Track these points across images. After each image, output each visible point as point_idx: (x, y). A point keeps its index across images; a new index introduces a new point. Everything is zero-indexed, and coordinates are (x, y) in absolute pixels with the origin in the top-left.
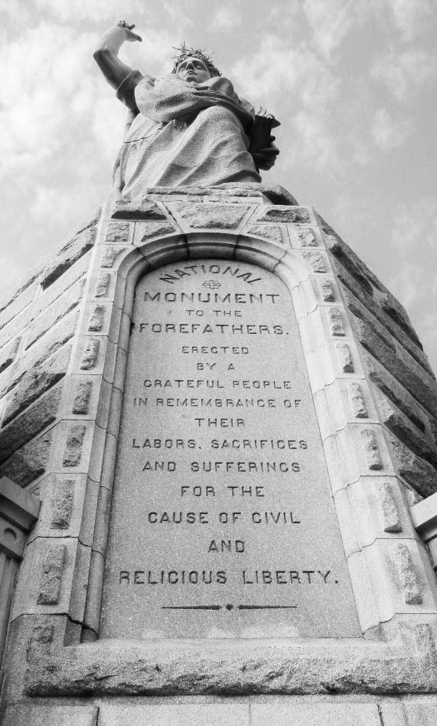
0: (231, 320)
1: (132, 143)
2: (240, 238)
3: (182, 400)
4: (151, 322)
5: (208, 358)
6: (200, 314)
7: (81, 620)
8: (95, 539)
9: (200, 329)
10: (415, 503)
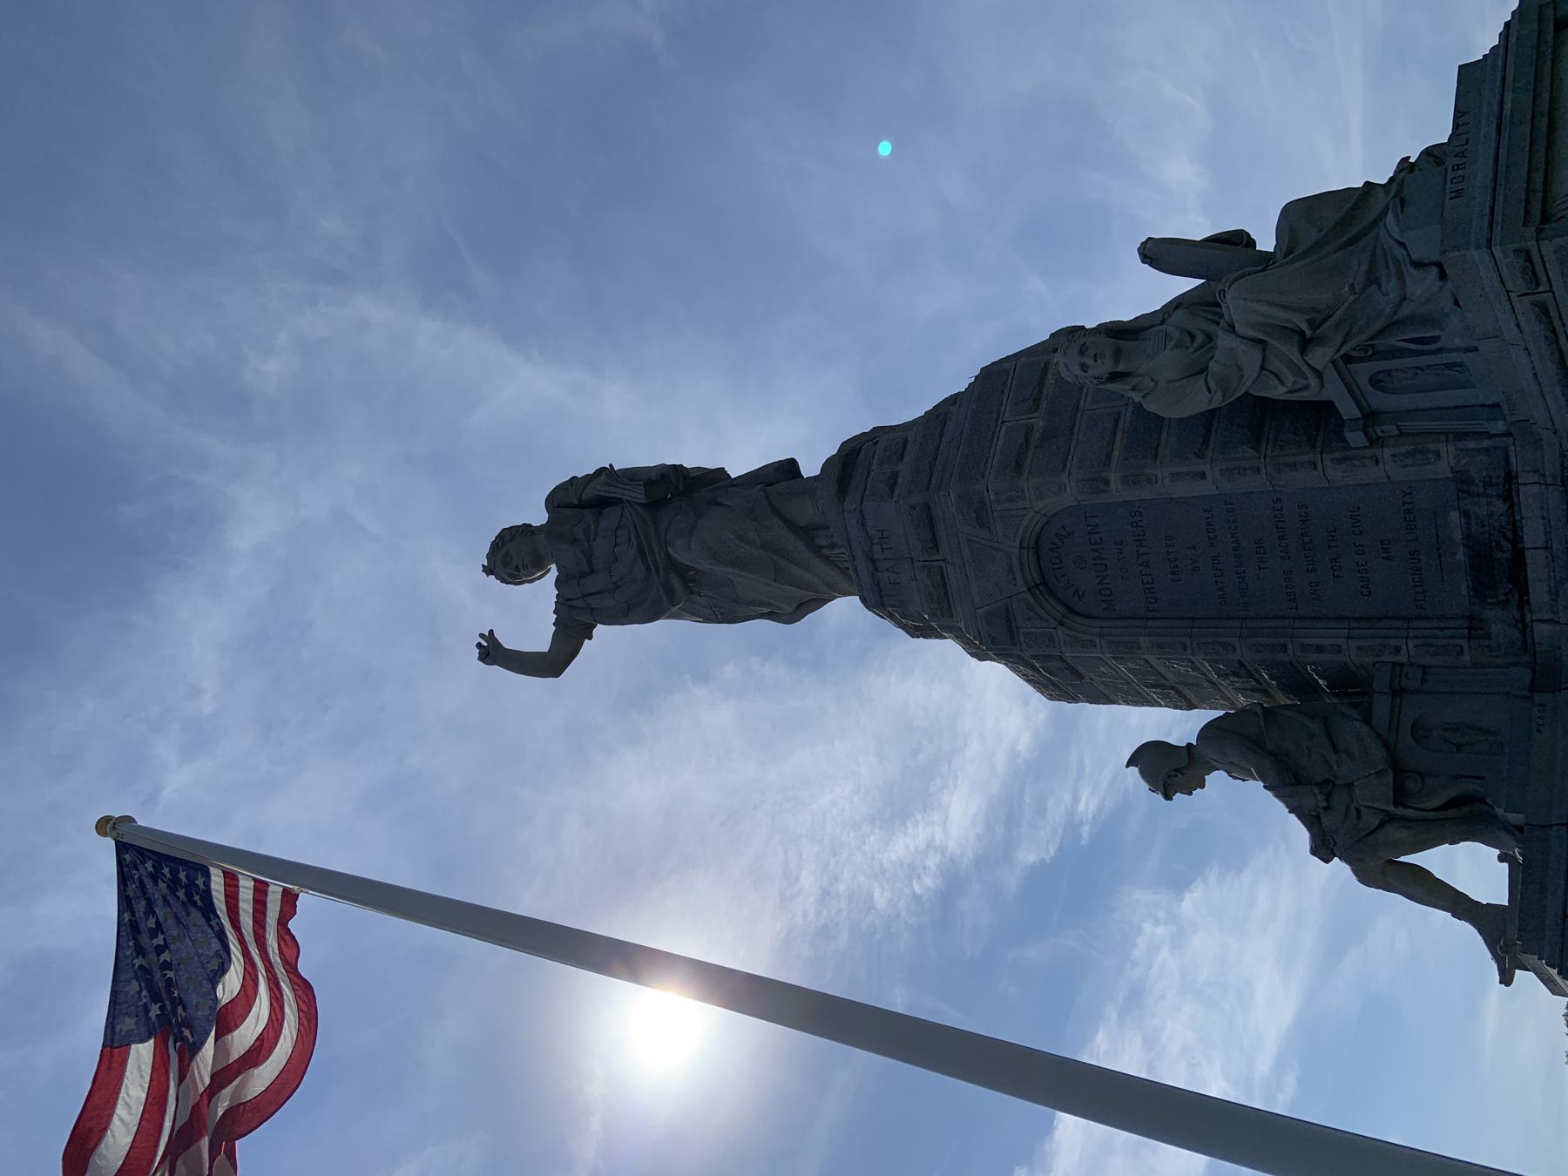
2: (1021, 547)
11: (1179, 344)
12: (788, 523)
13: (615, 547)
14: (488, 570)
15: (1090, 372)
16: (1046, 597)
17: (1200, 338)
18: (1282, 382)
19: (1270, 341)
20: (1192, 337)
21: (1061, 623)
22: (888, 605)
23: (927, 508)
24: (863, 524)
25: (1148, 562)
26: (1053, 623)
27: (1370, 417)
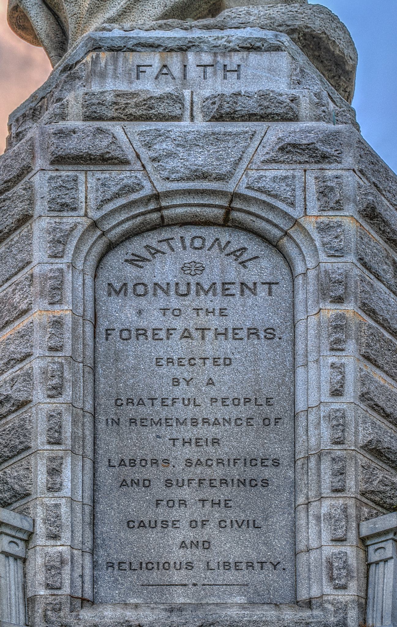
0: (215, 322)
3: (156, 420)
4: (118, 326)
5: (184, 372)
6: (177, 313)
7: (80, 596)
8: (83, 543)
9: (176, 336)
10: (367, 519)
16: (139, 220)
22: (98, 57)
25: (189, 337)
26: (96, 215)
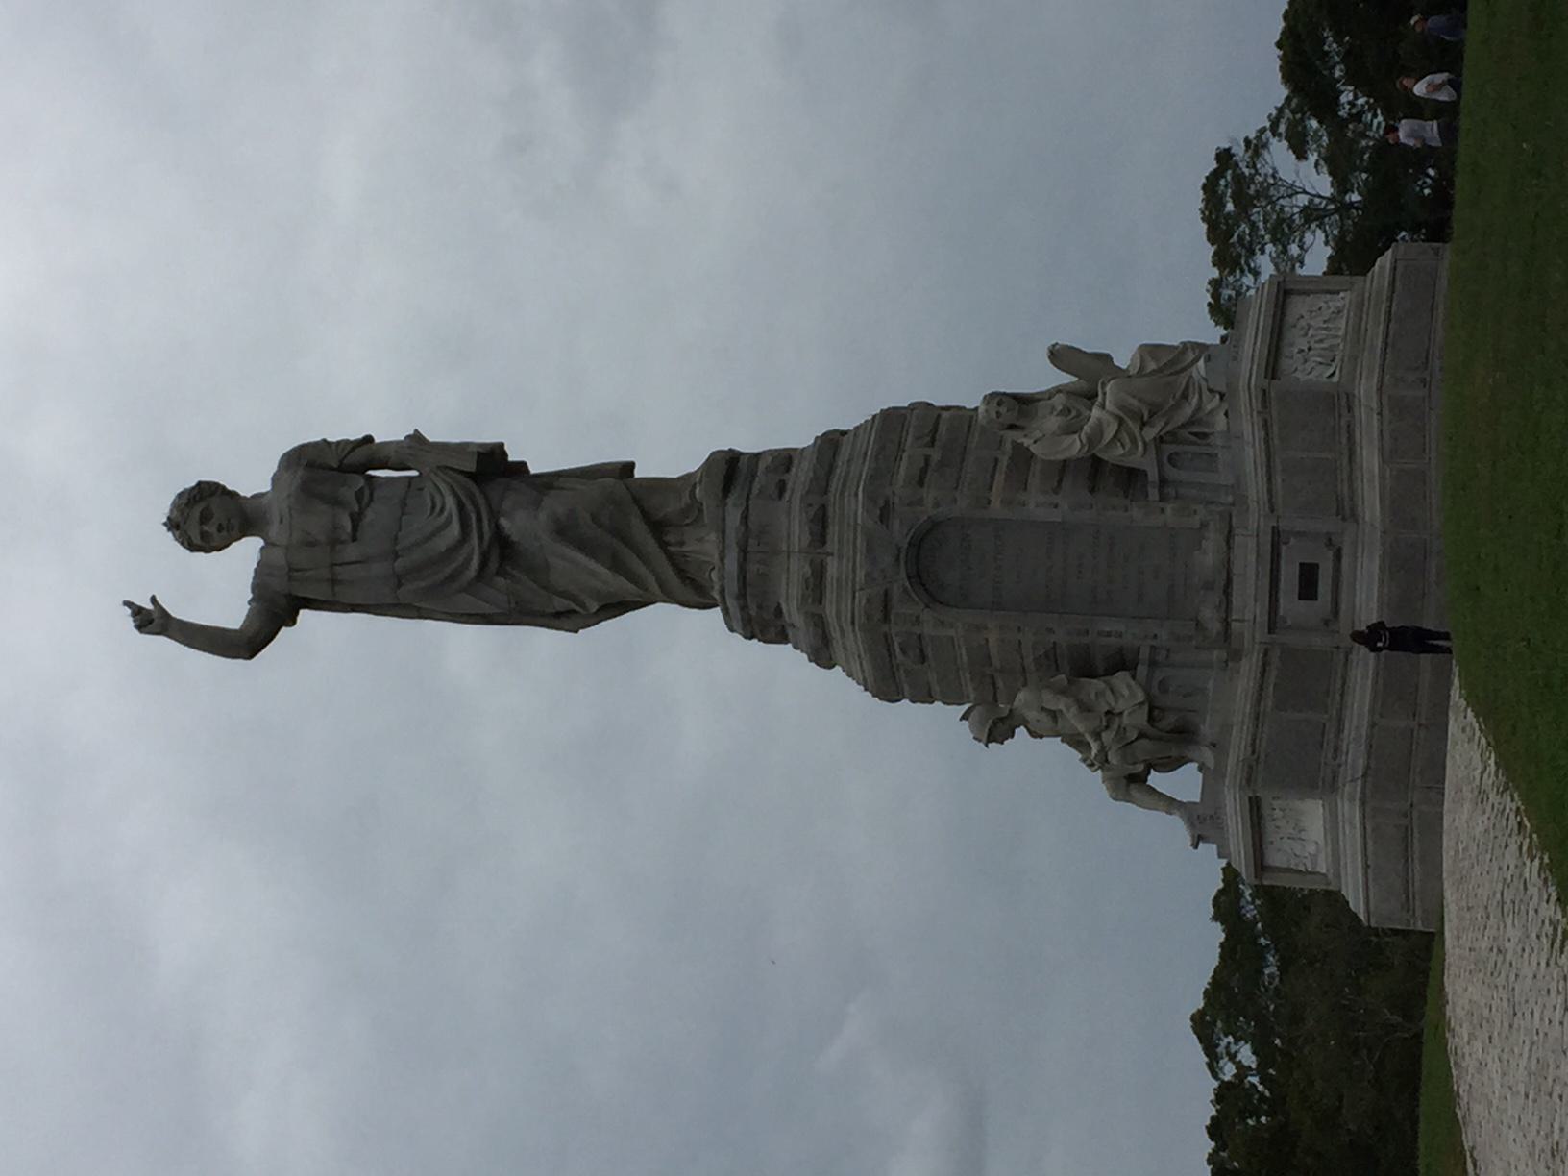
1: (513, 605)
11: (1061, 413)
12: (646, 515)
13: (403, 514)
14: (172, 525)
15: (1001, 420)
17: (1074, 413)
18: (1123, 446)
19: (1126, 418)
20: (1070, 411)
21: (927, 607)
23: (823, 508)
24: (745, 518)
26: (922, 606)
27: (1163, 482)
